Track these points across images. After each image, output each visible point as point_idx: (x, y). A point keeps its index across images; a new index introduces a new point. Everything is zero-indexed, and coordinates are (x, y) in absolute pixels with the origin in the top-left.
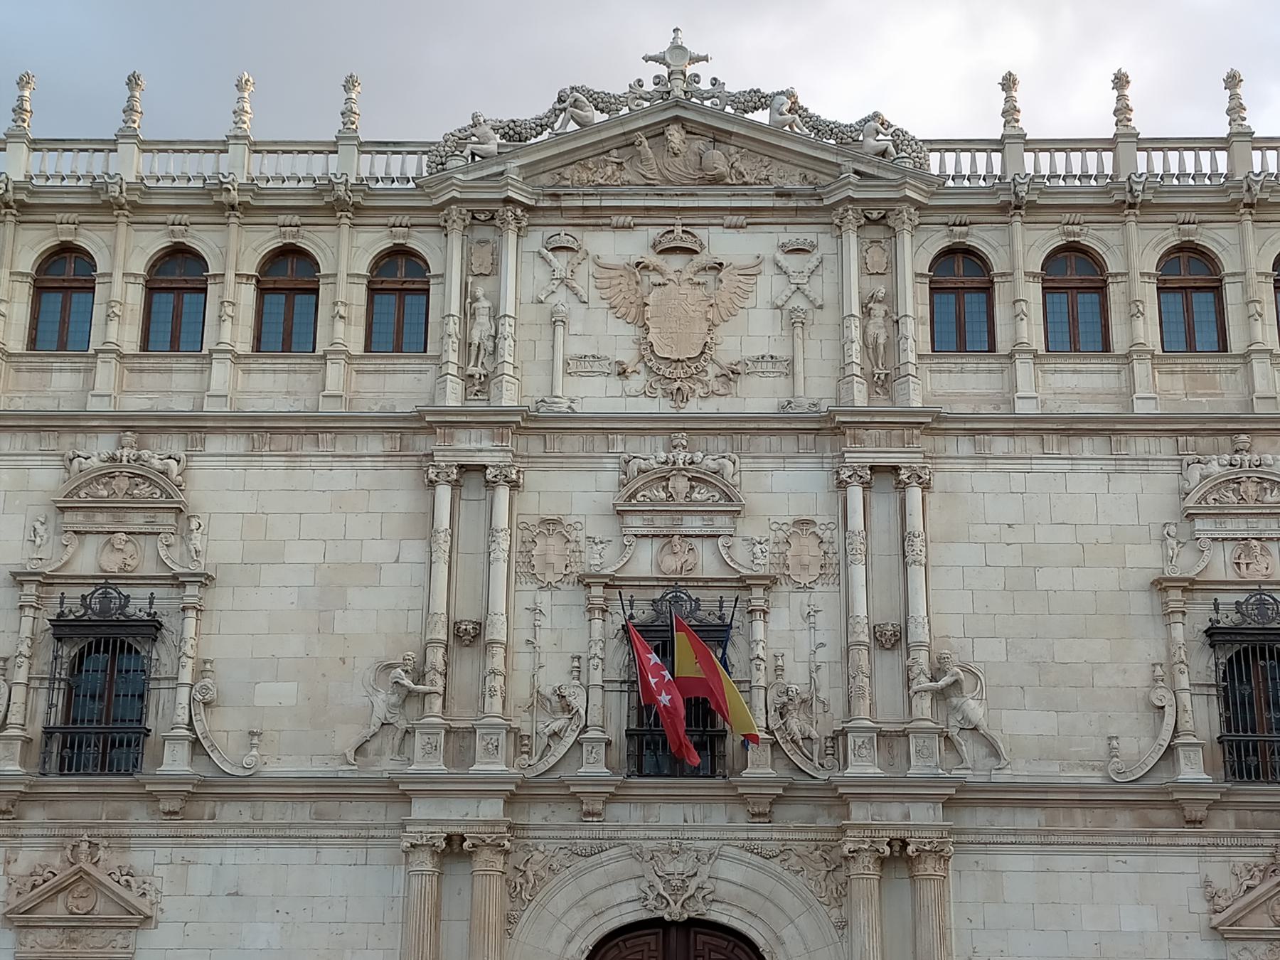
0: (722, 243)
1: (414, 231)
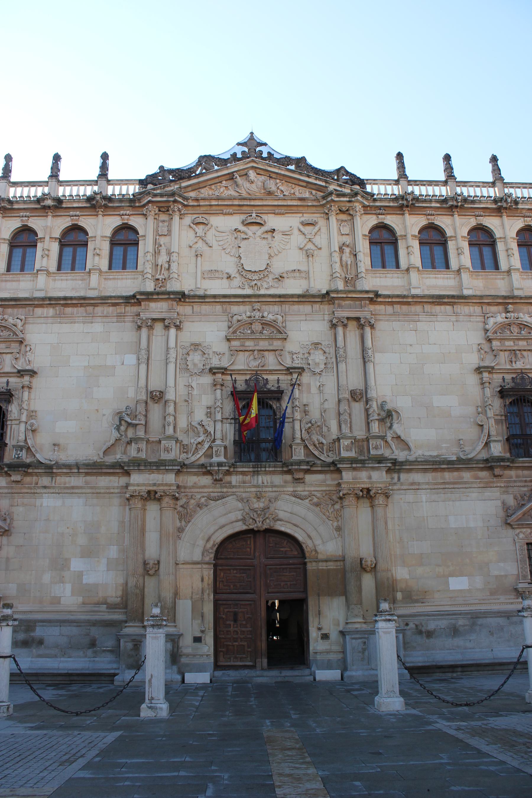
1: (132, 218)
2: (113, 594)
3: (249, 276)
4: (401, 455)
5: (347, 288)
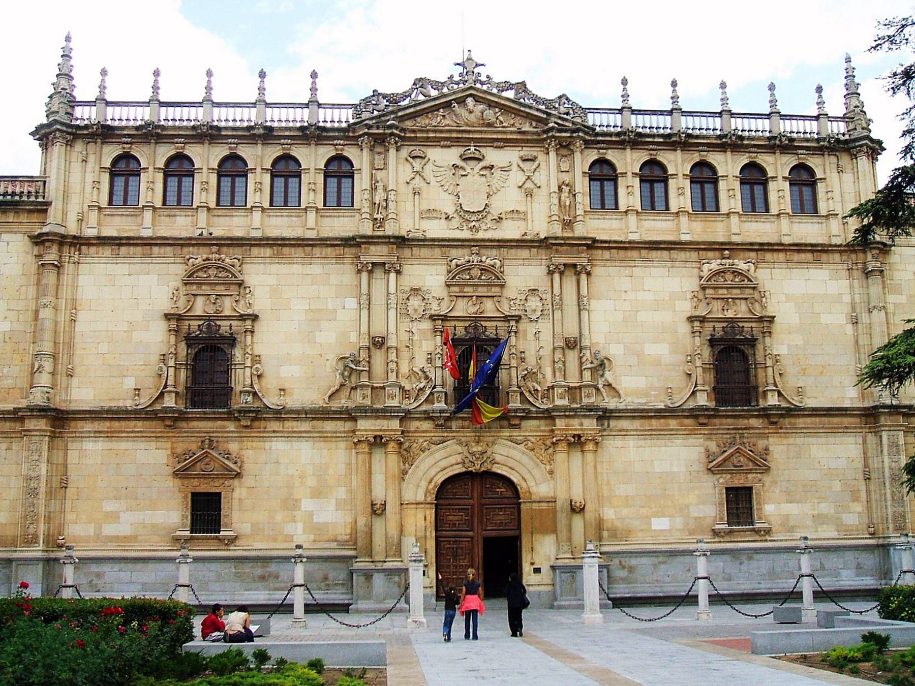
0: (492, 156)
1: (346, 148)
2: (343, 532)
3: (467, 216)
4: (612, 403)
5: (566, 235)
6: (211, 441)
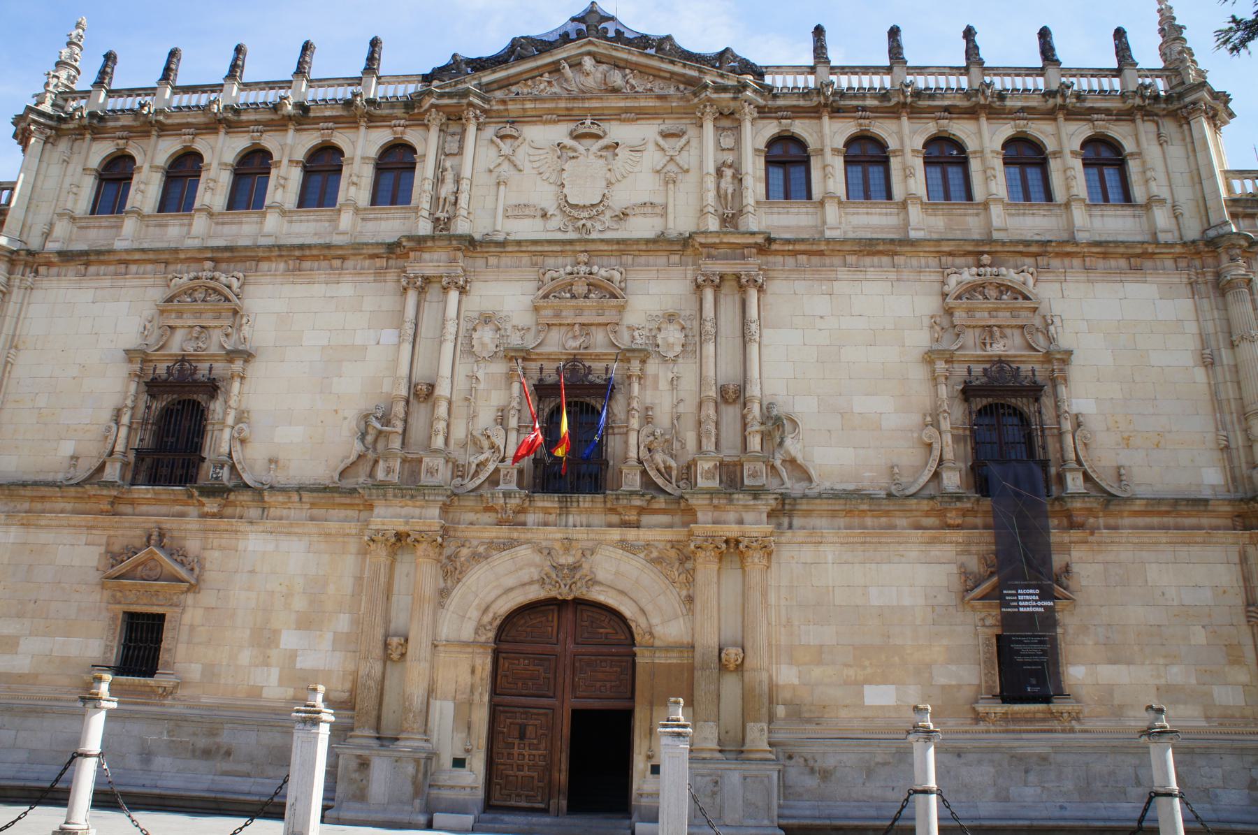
1: (408, 130)
3: (575, 213)
4: (794, 487)
6: (161, 536)
